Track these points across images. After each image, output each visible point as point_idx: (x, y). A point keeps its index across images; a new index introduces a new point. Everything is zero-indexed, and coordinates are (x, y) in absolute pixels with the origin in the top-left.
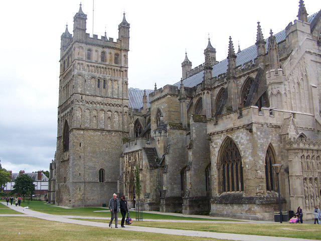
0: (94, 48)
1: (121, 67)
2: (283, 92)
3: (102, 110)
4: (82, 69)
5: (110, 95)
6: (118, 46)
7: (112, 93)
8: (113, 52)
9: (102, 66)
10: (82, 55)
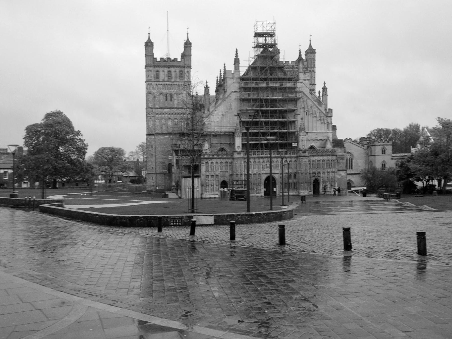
0: (161, 69)
1: (185, 82)
2: (206, 123)
3: (170, 119)
4: (151, 88)
5: (176, 106)
6: (182, 64)
7: (178, 105)
8: (178, 70)
9: (168, 83)
10: (151, 77)
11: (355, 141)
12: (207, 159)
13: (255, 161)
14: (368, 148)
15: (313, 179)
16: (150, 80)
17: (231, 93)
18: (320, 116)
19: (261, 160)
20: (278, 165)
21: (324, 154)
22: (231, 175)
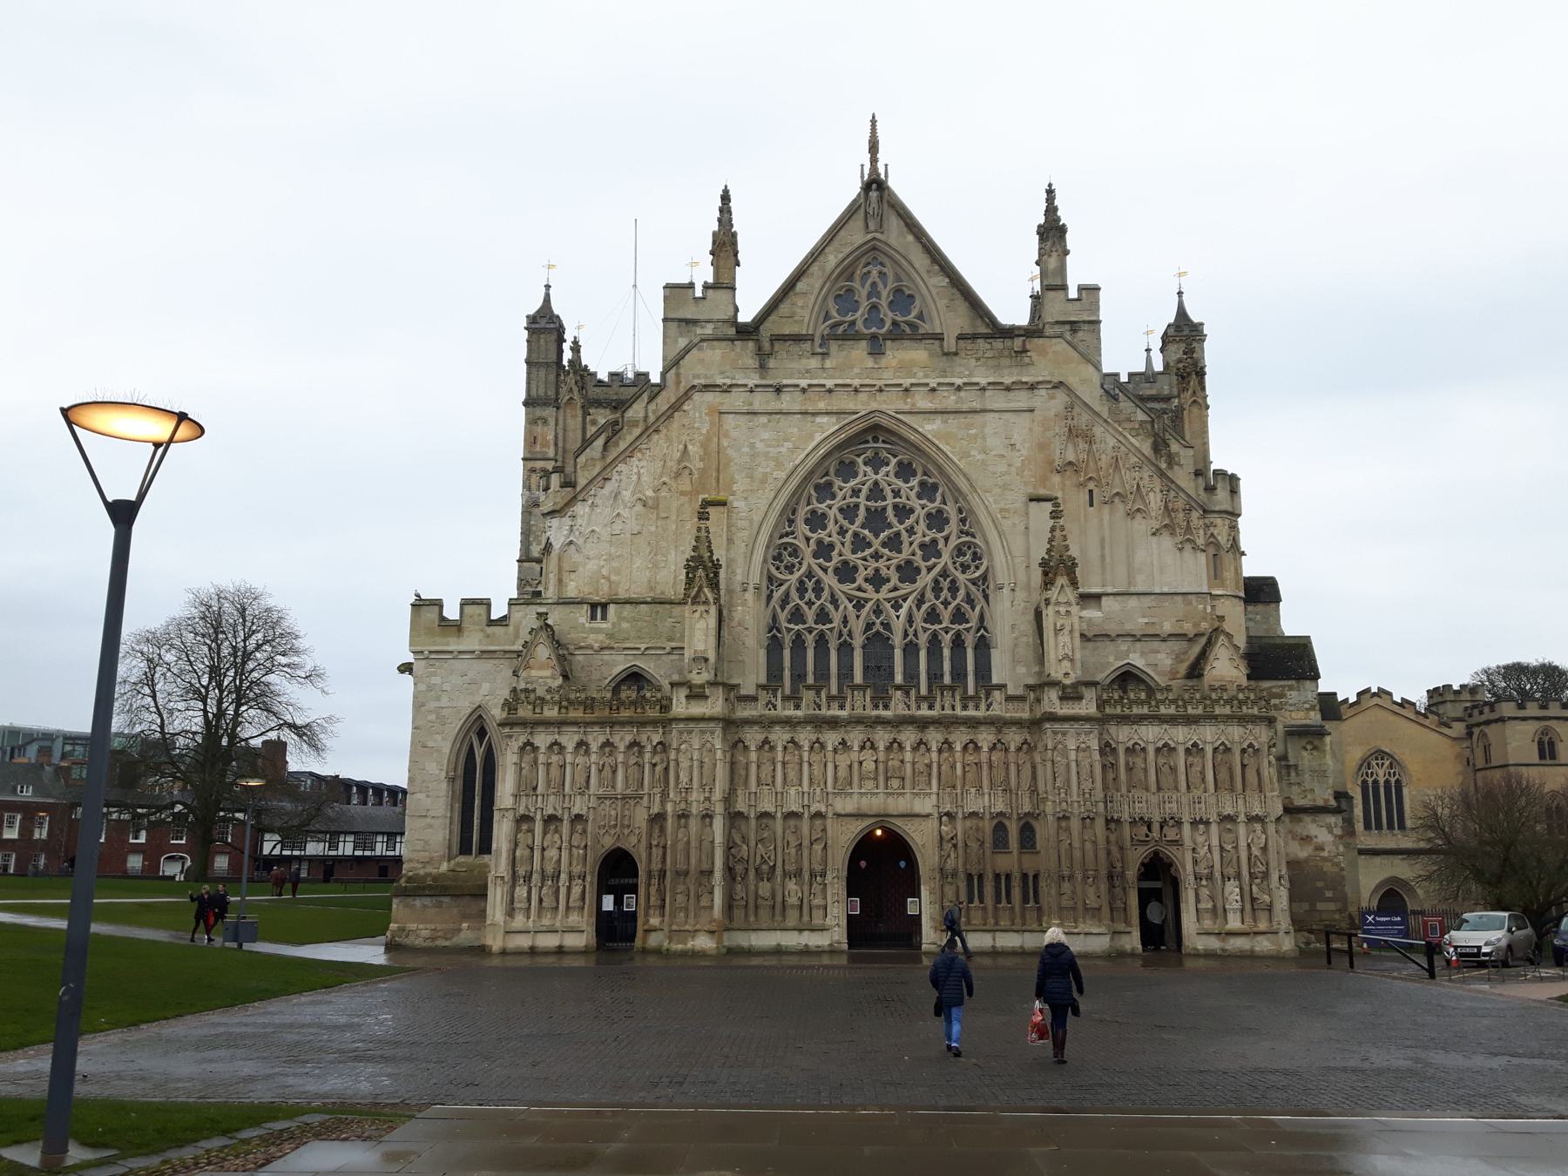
11: (1405, 703)
12: (523, 723)
13: (792, 741)
14: (1470, 735)
15: (1137, 856)
16: (539, 456)
17: (687, 395)
18: (1168, 510)
19: (831, 738)
20: (929, 766)
21: (1190, 711)
22: (658, 819)
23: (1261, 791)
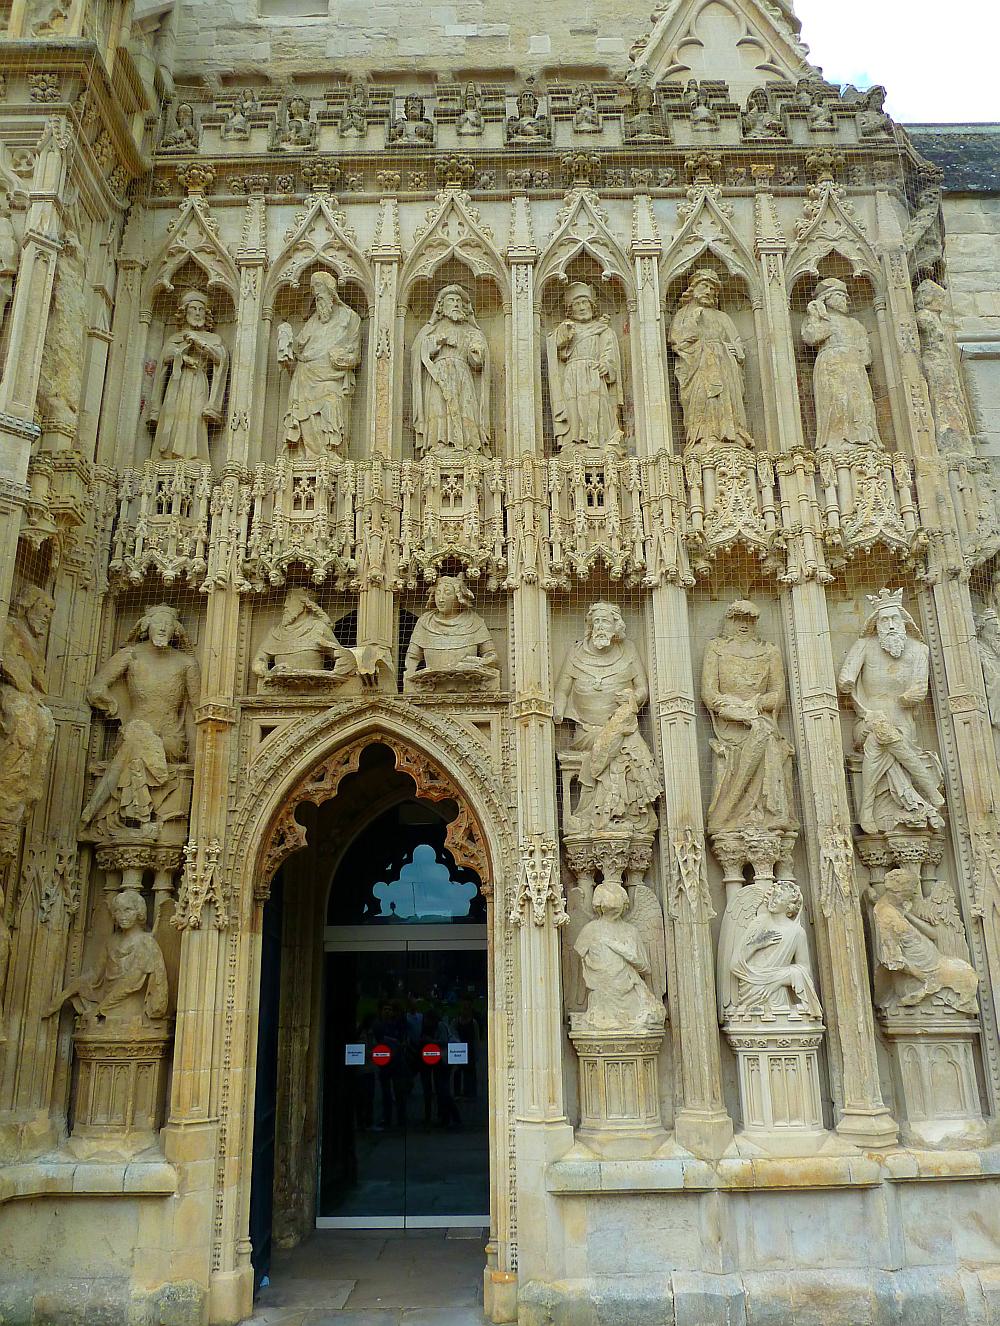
23: (891, 447)
